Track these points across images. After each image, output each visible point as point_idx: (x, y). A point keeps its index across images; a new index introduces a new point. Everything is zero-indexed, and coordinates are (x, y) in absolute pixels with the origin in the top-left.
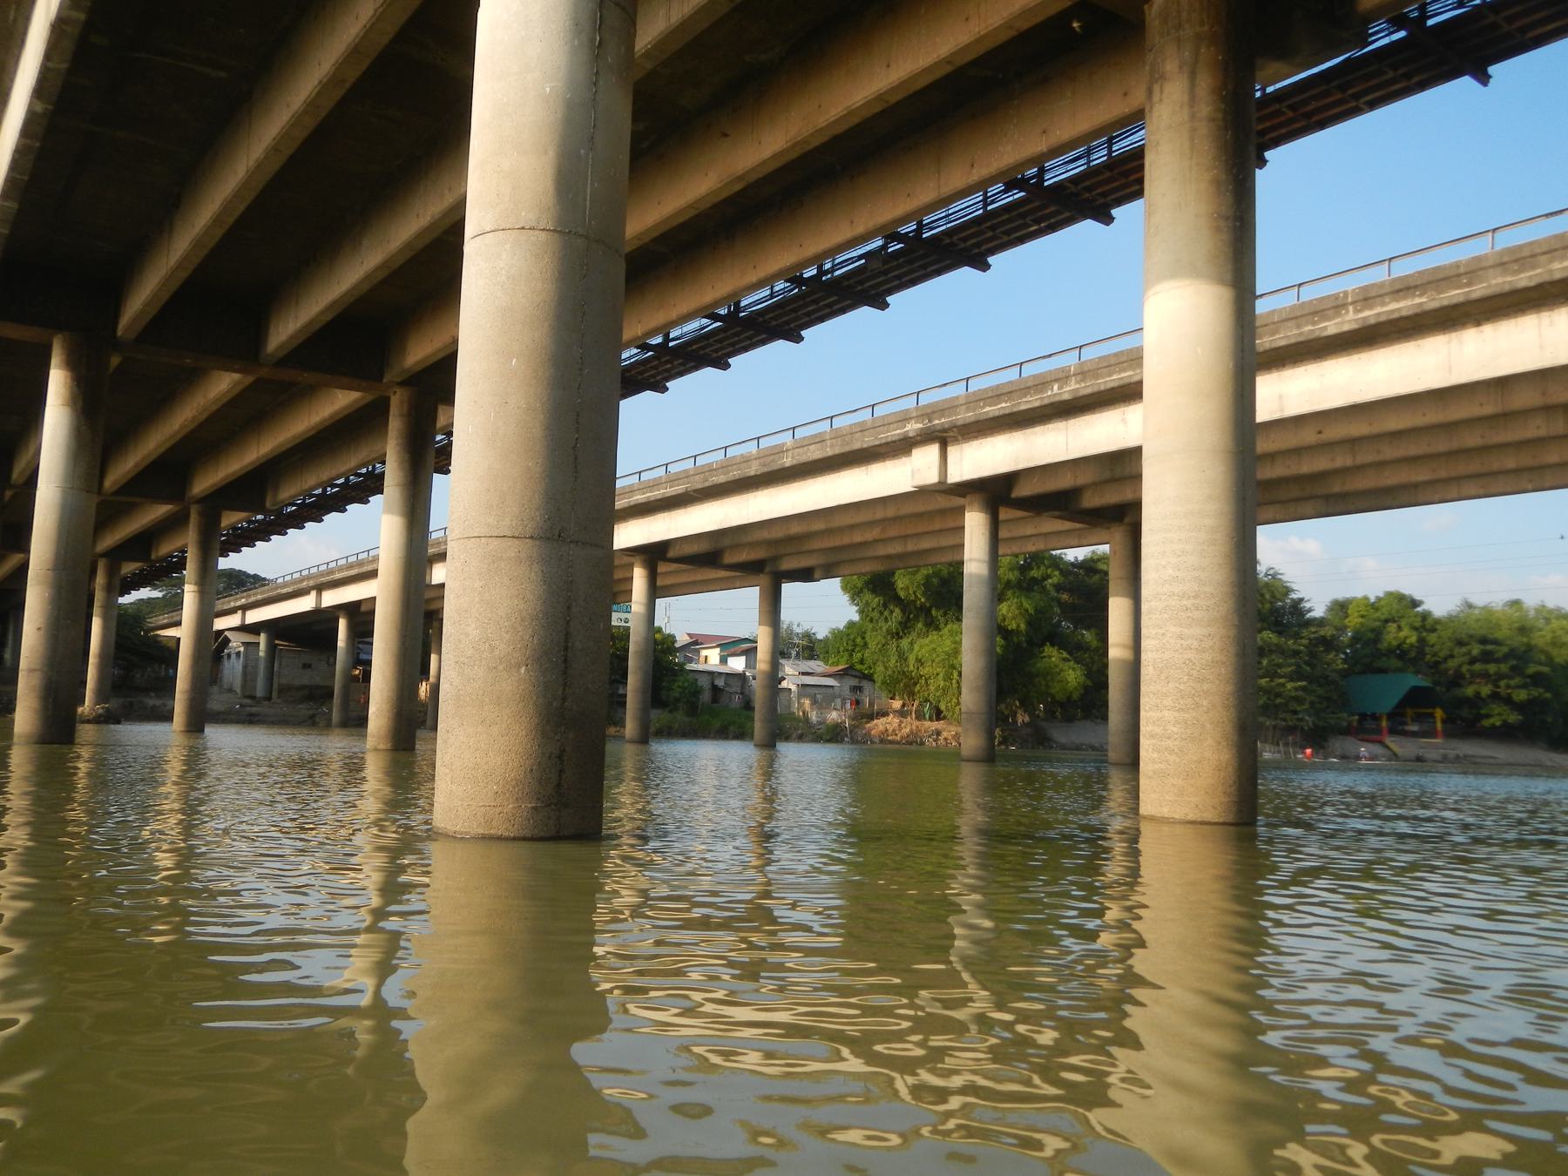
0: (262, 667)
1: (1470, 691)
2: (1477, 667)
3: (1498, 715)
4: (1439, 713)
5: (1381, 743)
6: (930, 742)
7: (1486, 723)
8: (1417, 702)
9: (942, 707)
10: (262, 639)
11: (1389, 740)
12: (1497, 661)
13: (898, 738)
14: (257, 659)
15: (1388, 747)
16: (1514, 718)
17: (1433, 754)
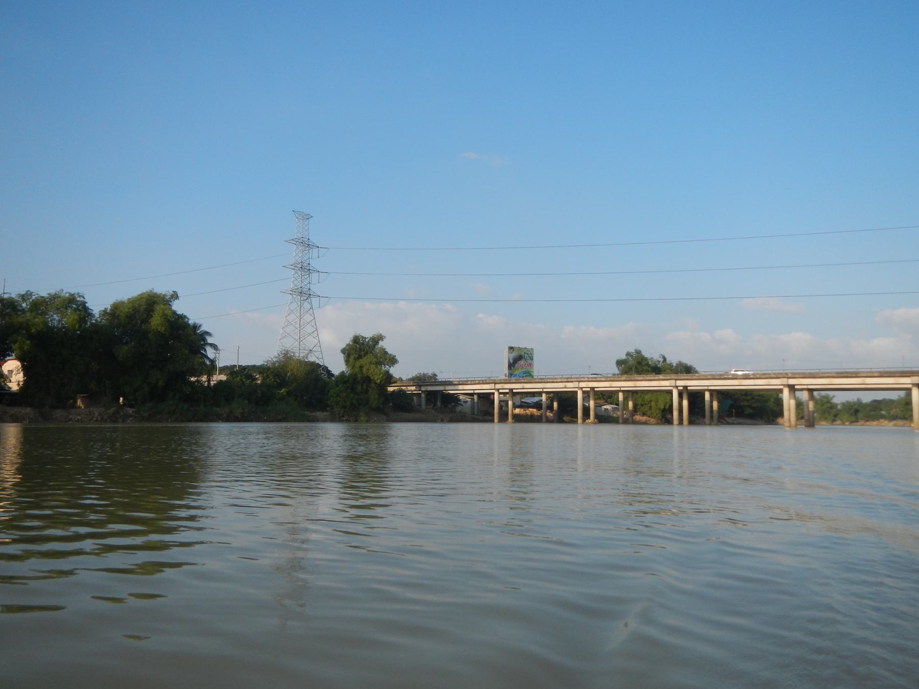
0: (476, 403)
1: (742, 404)
2: (744, 397)
3: (749, 411)
4: (734, 411)
5: (724, 419)
6: (648, 422)
7: (746, 413)
8: (732, 406)
9: (649, 413)
10: (475, 397)
11: (726, 419)
12: (748, 396)
13: (643, 422)
14: (474, 402)
15: (725, 420)
16: (752, 411)
17: (735, 422)
